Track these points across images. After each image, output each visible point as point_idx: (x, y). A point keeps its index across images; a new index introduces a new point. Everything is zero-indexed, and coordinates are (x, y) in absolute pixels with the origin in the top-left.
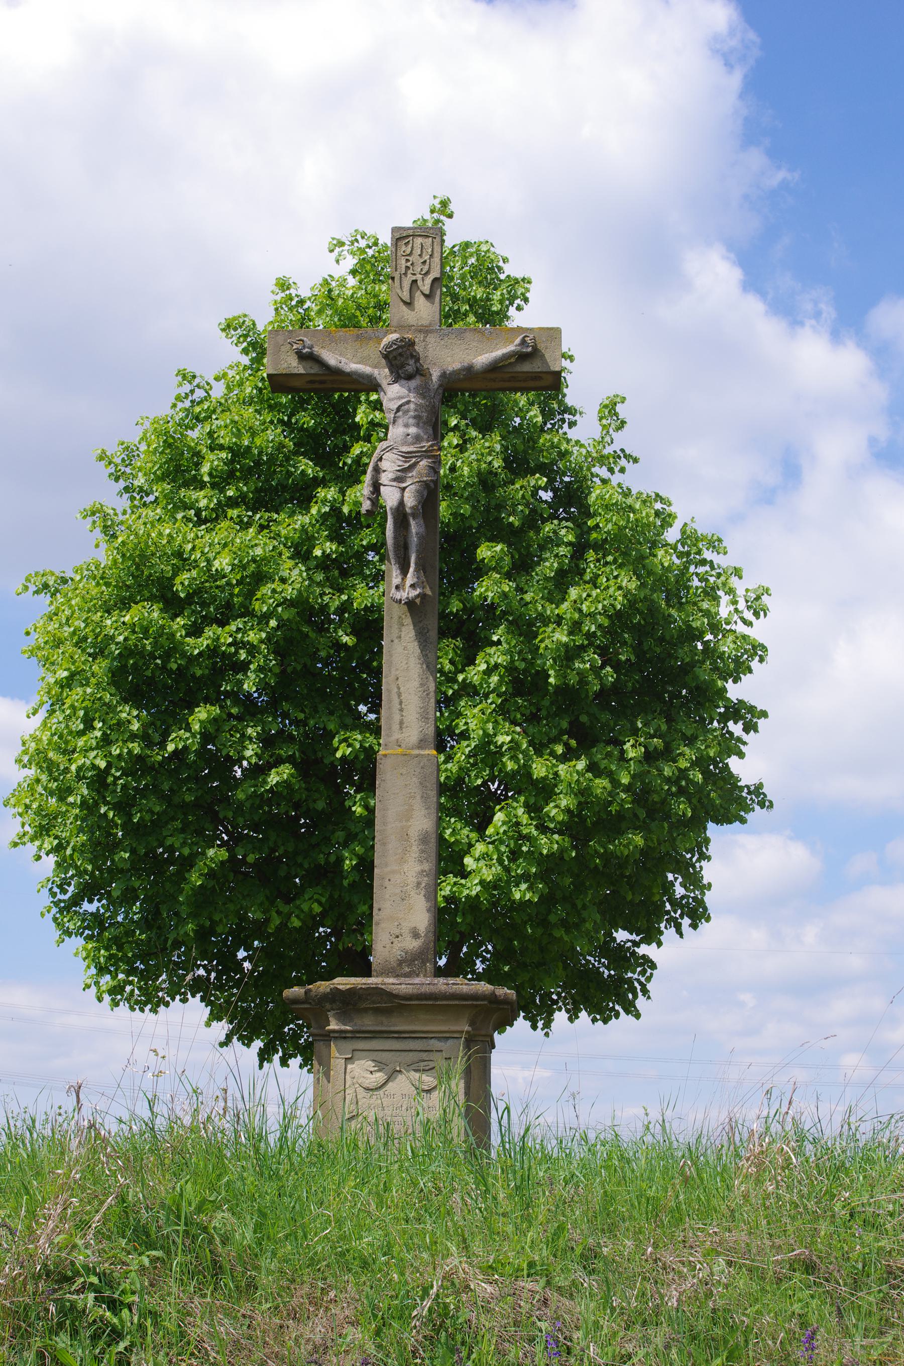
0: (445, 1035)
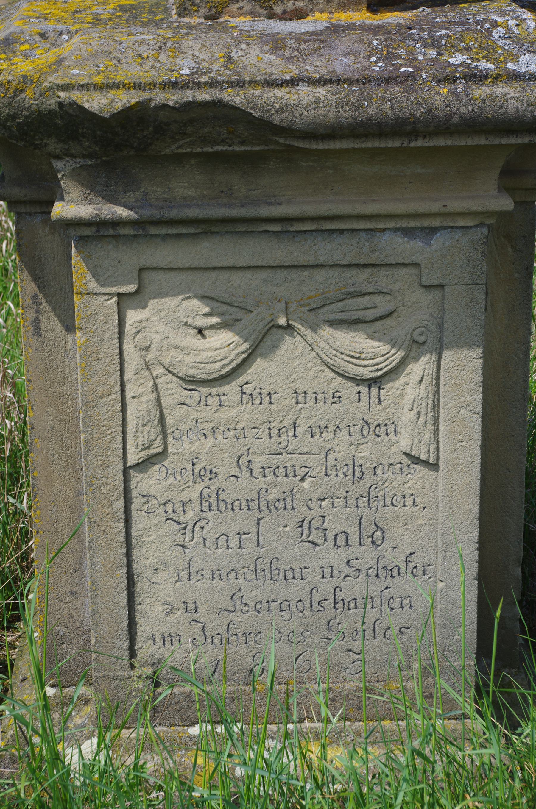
0: (426, 223)
